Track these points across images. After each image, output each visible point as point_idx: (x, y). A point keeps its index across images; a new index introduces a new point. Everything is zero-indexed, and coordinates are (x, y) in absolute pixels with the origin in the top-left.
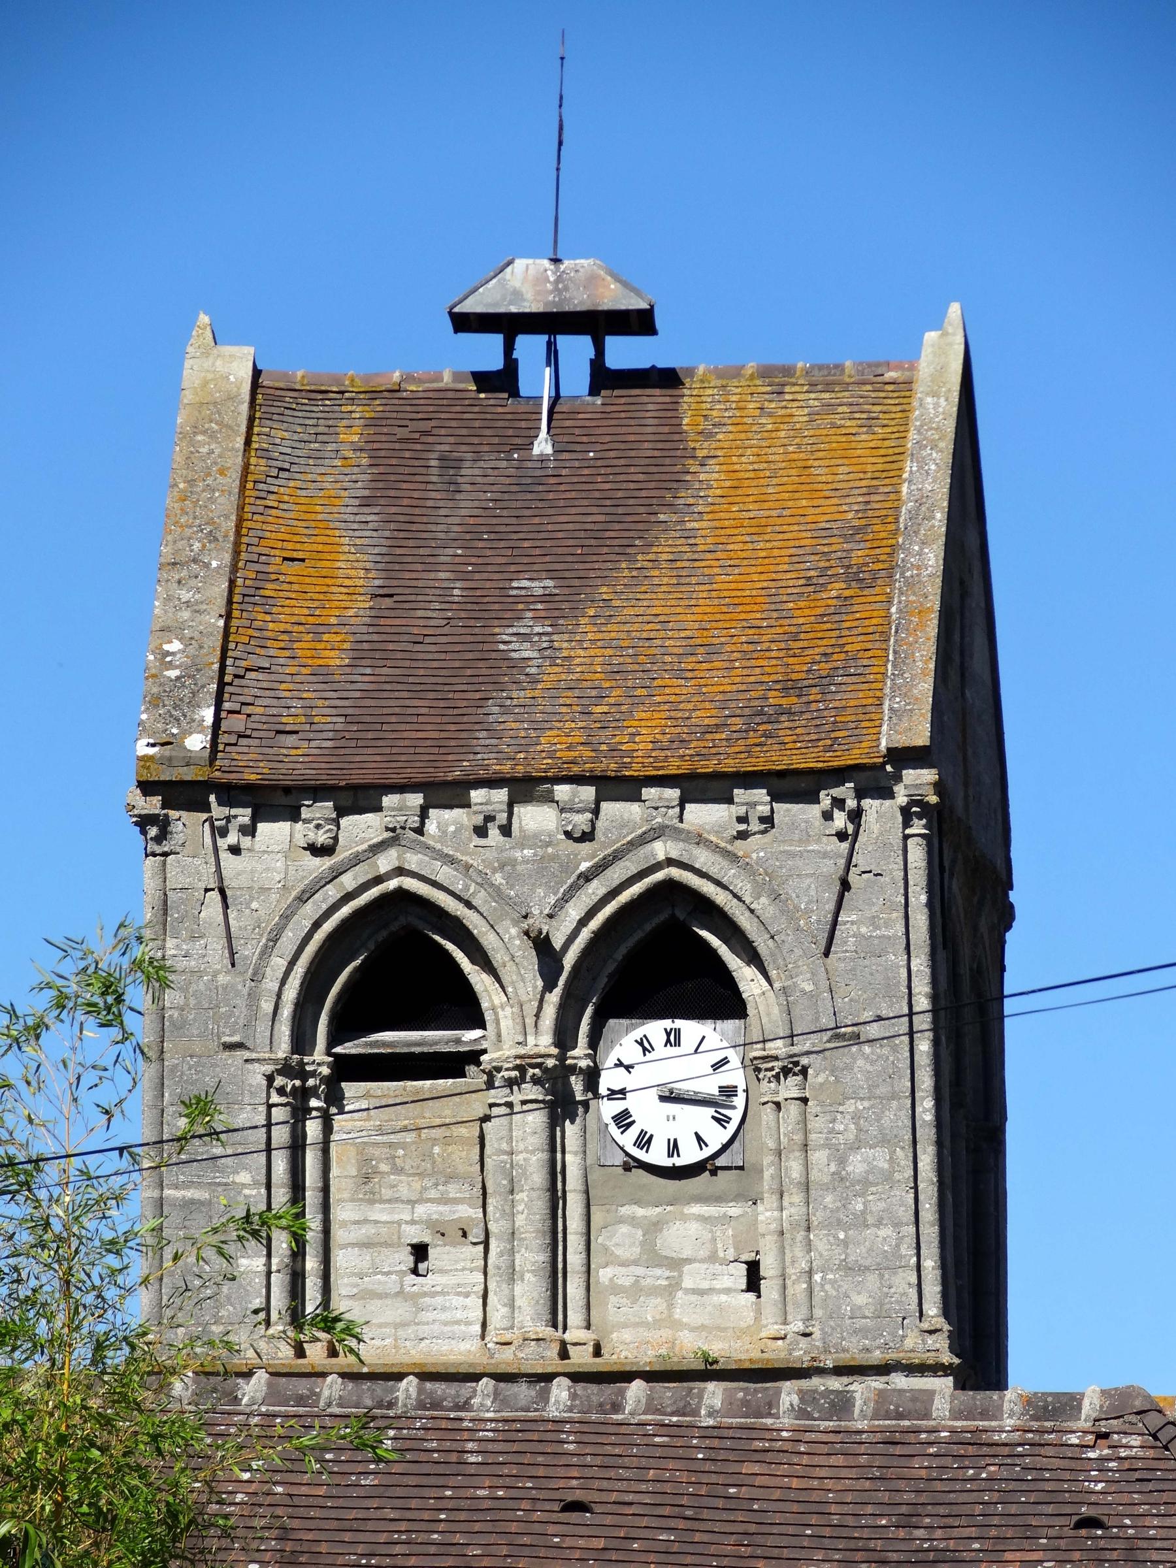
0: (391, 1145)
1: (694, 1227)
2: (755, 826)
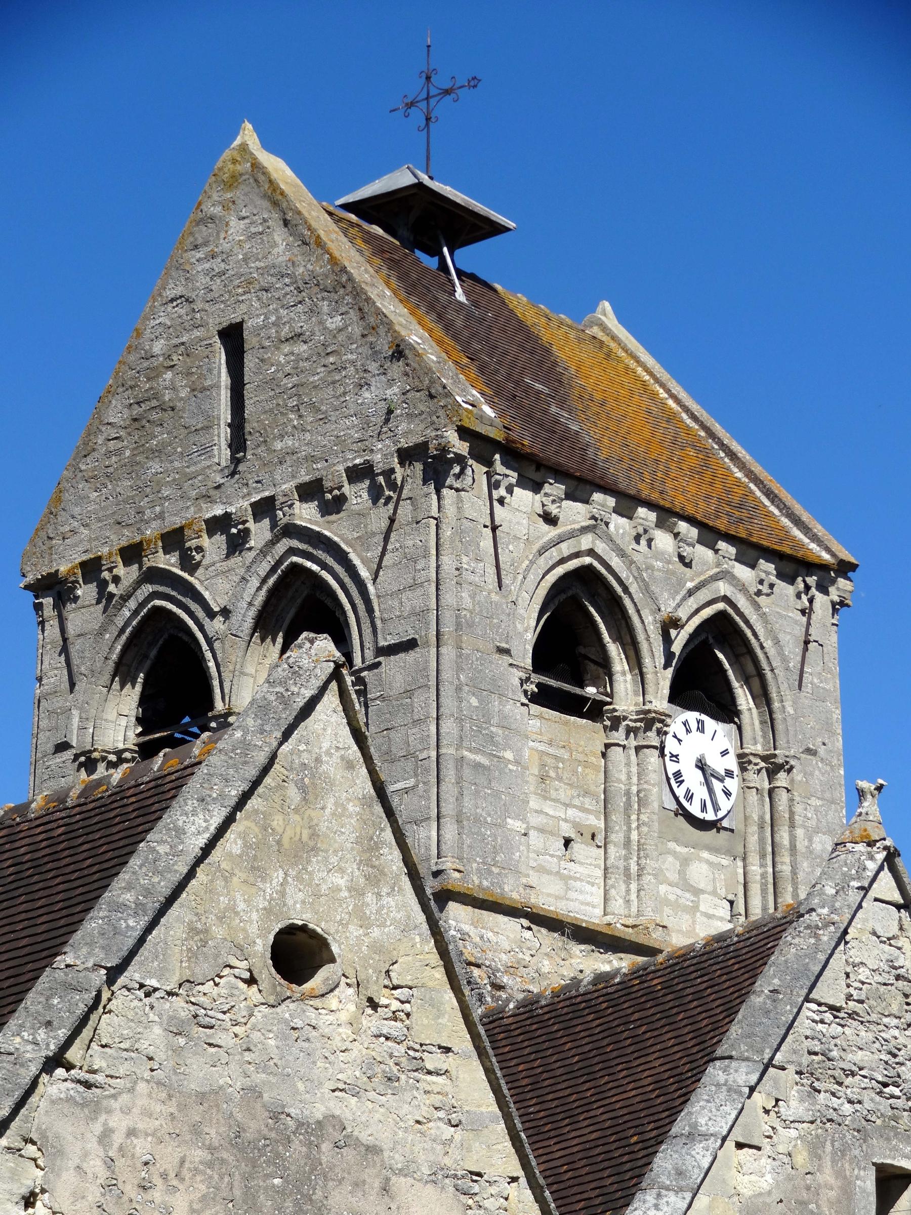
0: (556, 758)
1: (705, 867)
2: (765, 589)
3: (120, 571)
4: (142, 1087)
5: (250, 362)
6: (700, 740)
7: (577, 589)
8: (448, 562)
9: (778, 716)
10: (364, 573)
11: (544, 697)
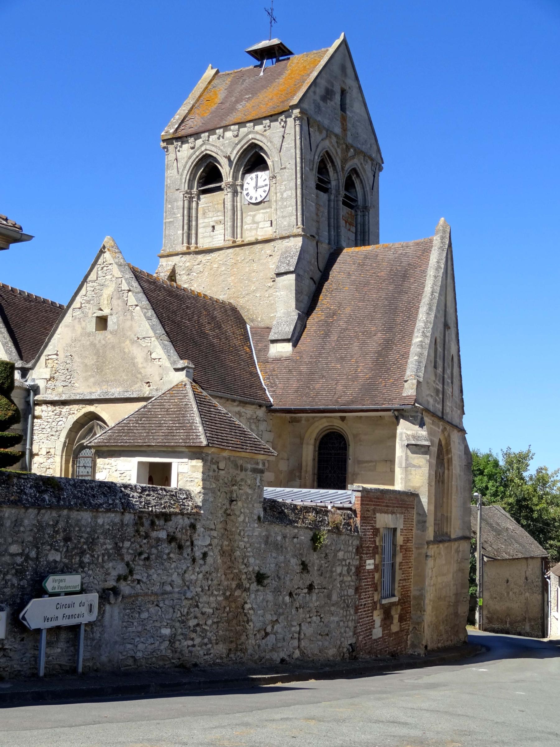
1: (261, 215)
2: (267, 128)
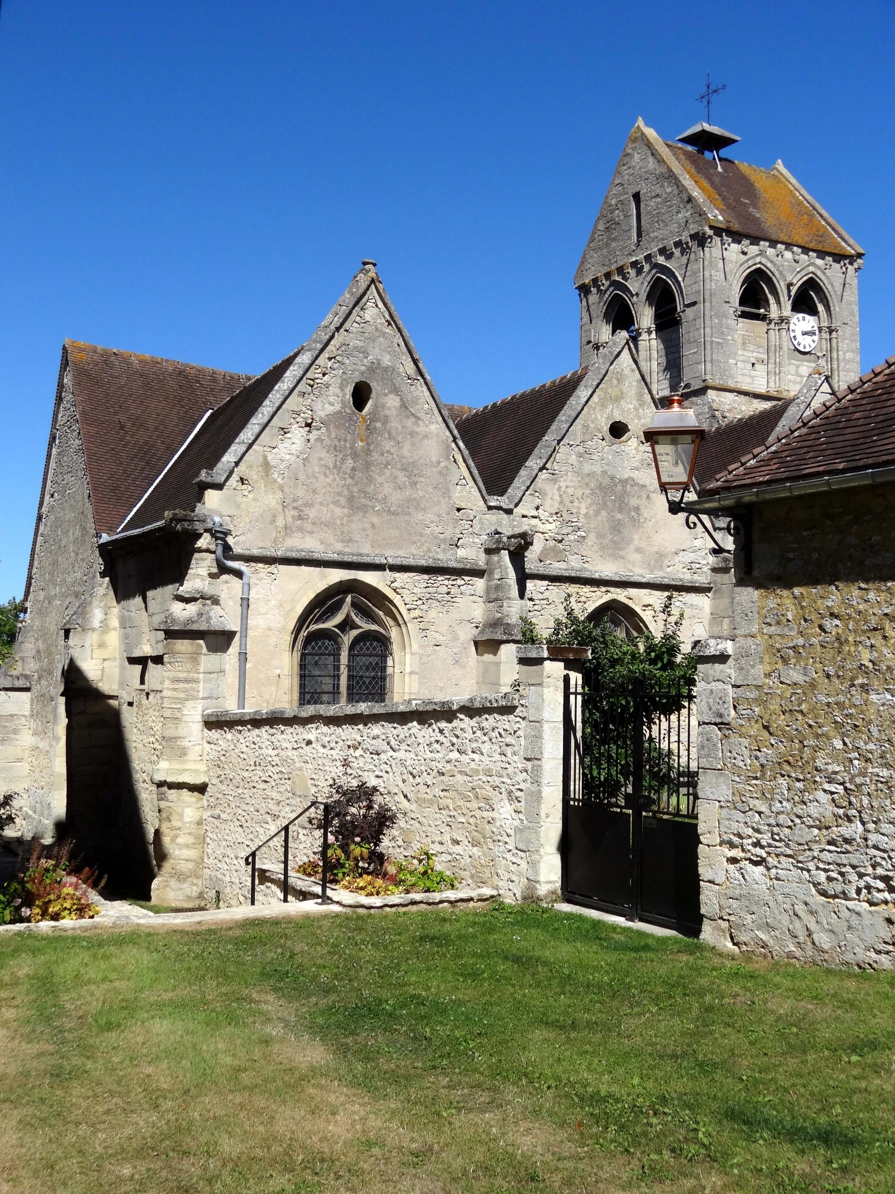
2: (828, 267)
3: (604, 281)
4: (570, 474)
5: (642, 206)
6: (802, 323)
7: (756, 276)
8: (707, 273)
9: (833, 312)
10: (680, 279)
11: (744, 315)
